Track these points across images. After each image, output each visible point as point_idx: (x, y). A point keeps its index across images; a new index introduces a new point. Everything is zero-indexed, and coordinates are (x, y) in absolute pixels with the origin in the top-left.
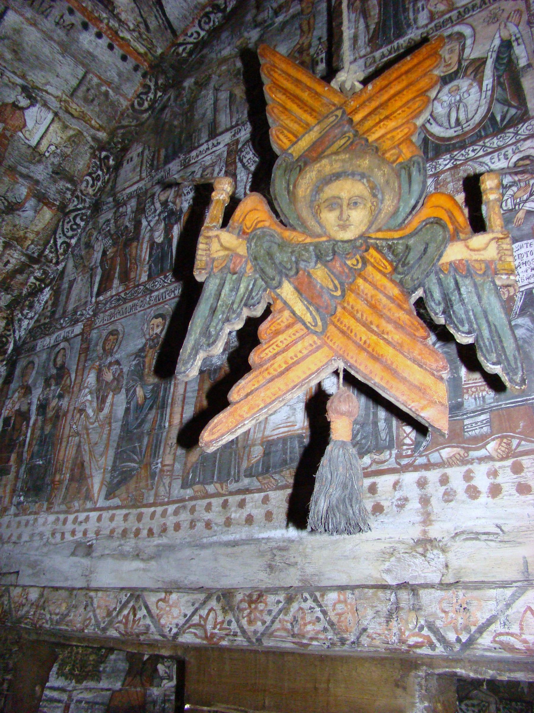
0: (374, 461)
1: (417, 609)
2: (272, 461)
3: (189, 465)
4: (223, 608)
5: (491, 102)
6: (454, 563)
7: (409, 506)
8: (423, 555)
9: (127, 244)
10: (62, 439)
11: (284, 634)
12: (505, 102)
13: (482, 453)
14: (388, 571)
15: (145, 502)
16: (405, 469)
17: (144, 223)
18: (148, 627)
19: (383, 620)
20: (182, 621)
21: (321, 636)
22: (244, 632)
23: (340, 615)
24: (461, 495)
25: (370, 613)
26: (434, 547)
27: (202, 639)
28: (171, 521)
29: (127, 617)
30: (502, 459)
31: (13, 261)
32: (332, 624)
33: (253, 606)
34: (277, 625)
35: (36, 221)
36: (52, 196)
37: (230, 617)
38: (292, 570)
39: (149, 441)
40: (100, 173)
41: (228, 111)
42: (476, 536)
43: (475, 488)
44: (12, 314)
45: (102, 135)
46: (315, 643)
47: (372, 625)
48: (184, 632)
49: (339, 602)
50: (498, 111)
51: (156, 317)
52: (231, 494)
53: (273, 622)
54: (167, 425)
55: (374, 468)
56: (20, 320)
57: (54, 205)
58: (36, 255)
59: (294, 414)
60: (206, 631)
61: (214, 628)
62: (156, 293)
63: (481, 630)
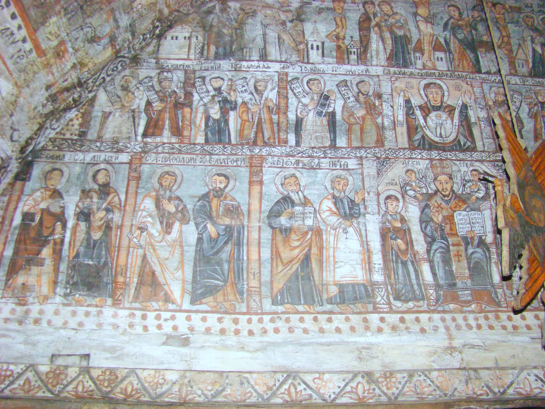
0: (415, 306)
1: (478, 378)
2: (346, 296)
3: (275, 290)
4: (367, 382)
5: (458, 133)
6: (466, 358)
7: (439, 330)
8: (451, 354)
9: (178, 105)
10: (119, 247)
11: (412, 393)
12: (465, 137)
13: (469, 309)
14: (434, 361)
15: (237, 311)
16: (433, 311)
17: (196, 97)
18: (311, 396)
19: (464, 384)
20: (337, 390)
21: (434, 393)
22: (385, 394)
23: (441, 382)
24: (464, 327)
25: (457, 382)
26: (456, 351)
27: (356, 400)
28: (270, 327)
29: (289, 390)
30: (479, 313)
31: (70, 80)
32: (438, 387)
33: (388, 380)
34: (406, 389)
35: (100, 56)
36: (119, 42)
37: (373, 386)
38: (375, 360)
39: (229, 267)
40: (148, 36)
41: (278, 48)
42: (473, 346)
43: (469, 325)
44: (45, 122)
45: (166, 11)
46: (430, 397)
47: (459, 387)
48: (342, 397)
49: (439, 376)
50: (462, 140)
51: (219, 175)
52: (318, 313)
53: (403, 388)
54: (245, 258)
55: (415, 309)
56: (47, 128)
57: (115, 48)
58: (83, 81)
59: (354, 271)
60: (358, 395)
61: (364, 393)
62: (217, 157)
63: (509, 387)
